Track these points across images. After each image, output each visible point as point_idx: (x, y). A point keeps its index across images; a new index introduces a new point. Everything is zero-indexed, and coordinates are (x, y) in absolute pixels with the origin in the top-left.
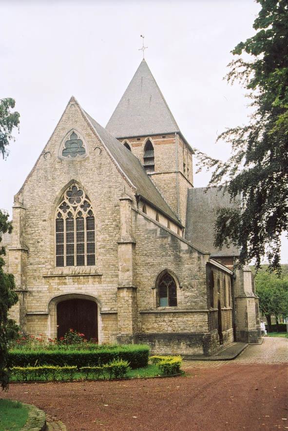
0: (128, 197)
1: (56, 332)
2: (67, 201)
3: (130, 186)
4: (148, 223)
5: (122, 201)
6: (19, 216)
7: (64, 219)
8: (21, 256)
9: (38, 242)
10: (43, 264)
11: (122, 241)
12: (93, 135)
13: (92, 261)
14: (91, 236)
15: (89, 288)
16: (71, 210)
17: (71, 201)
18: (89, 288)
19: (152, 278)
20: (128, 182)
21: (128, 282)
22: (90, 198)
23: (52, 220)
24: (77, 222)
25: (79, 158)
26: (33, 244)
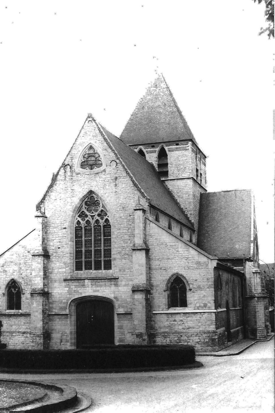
13: (108, 266)
18: (105, 291)
24: (95, 229)
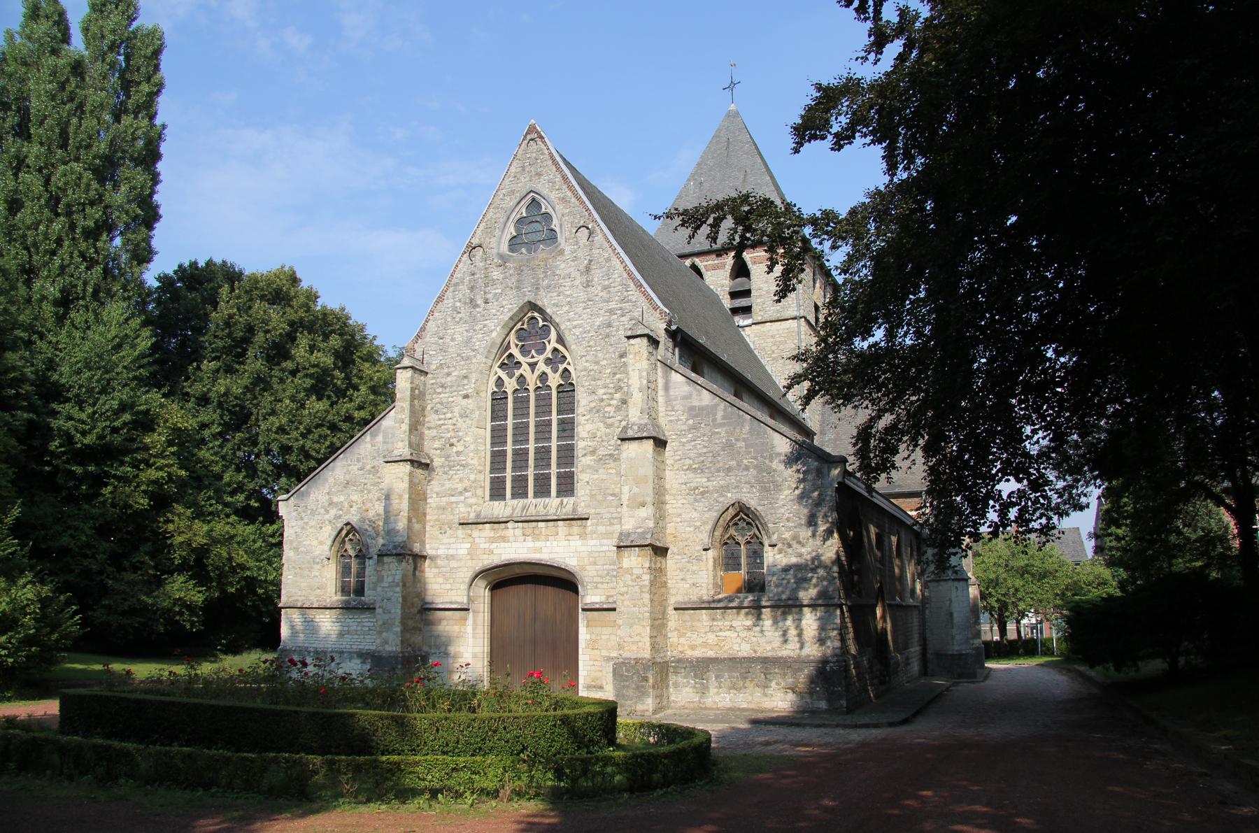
0: (646, 331)
1: (487, 649)
2: (515, 351)
3: (656, 308)
4: (695, 393)
5: (632, 341)
6: (409, 386)
7: (509, 391)
8: (411, 474)
9: (452, 445)
10: (461, 493)
11: (630, 434)
12: (573, 200)
13: (567, 486)
14: (567, 428)
15: (557, 549)
16: (525, 370)
17: (524, 351)
18: (555, 549)
19: (704, 523)
20: (650, 300)
21: (643, 533)
22: (568, 338)
23: (483, 394)
24: (538, 398)
25: (542, 252)
26: (442, 449)
